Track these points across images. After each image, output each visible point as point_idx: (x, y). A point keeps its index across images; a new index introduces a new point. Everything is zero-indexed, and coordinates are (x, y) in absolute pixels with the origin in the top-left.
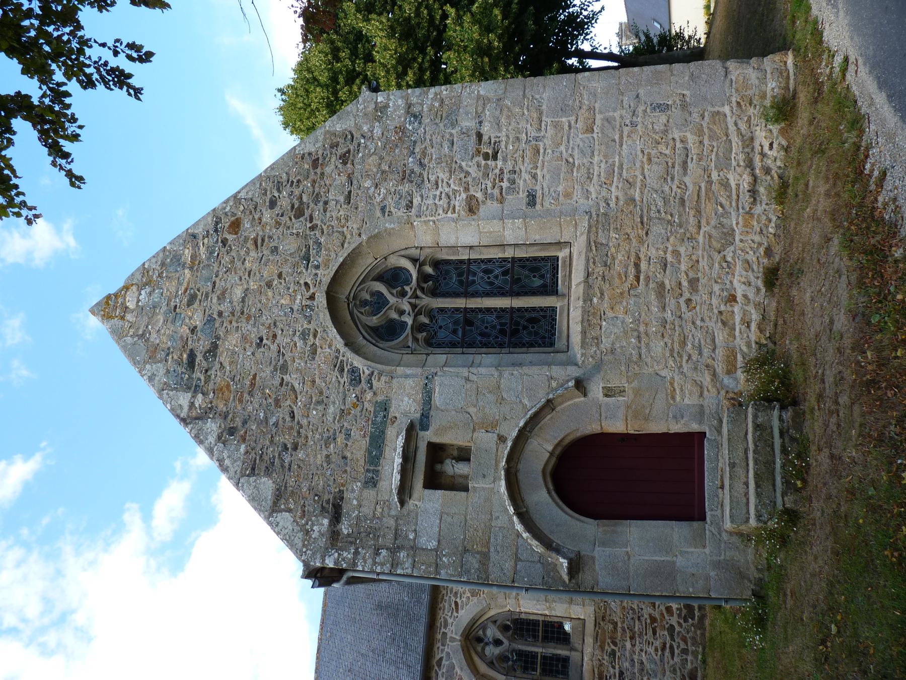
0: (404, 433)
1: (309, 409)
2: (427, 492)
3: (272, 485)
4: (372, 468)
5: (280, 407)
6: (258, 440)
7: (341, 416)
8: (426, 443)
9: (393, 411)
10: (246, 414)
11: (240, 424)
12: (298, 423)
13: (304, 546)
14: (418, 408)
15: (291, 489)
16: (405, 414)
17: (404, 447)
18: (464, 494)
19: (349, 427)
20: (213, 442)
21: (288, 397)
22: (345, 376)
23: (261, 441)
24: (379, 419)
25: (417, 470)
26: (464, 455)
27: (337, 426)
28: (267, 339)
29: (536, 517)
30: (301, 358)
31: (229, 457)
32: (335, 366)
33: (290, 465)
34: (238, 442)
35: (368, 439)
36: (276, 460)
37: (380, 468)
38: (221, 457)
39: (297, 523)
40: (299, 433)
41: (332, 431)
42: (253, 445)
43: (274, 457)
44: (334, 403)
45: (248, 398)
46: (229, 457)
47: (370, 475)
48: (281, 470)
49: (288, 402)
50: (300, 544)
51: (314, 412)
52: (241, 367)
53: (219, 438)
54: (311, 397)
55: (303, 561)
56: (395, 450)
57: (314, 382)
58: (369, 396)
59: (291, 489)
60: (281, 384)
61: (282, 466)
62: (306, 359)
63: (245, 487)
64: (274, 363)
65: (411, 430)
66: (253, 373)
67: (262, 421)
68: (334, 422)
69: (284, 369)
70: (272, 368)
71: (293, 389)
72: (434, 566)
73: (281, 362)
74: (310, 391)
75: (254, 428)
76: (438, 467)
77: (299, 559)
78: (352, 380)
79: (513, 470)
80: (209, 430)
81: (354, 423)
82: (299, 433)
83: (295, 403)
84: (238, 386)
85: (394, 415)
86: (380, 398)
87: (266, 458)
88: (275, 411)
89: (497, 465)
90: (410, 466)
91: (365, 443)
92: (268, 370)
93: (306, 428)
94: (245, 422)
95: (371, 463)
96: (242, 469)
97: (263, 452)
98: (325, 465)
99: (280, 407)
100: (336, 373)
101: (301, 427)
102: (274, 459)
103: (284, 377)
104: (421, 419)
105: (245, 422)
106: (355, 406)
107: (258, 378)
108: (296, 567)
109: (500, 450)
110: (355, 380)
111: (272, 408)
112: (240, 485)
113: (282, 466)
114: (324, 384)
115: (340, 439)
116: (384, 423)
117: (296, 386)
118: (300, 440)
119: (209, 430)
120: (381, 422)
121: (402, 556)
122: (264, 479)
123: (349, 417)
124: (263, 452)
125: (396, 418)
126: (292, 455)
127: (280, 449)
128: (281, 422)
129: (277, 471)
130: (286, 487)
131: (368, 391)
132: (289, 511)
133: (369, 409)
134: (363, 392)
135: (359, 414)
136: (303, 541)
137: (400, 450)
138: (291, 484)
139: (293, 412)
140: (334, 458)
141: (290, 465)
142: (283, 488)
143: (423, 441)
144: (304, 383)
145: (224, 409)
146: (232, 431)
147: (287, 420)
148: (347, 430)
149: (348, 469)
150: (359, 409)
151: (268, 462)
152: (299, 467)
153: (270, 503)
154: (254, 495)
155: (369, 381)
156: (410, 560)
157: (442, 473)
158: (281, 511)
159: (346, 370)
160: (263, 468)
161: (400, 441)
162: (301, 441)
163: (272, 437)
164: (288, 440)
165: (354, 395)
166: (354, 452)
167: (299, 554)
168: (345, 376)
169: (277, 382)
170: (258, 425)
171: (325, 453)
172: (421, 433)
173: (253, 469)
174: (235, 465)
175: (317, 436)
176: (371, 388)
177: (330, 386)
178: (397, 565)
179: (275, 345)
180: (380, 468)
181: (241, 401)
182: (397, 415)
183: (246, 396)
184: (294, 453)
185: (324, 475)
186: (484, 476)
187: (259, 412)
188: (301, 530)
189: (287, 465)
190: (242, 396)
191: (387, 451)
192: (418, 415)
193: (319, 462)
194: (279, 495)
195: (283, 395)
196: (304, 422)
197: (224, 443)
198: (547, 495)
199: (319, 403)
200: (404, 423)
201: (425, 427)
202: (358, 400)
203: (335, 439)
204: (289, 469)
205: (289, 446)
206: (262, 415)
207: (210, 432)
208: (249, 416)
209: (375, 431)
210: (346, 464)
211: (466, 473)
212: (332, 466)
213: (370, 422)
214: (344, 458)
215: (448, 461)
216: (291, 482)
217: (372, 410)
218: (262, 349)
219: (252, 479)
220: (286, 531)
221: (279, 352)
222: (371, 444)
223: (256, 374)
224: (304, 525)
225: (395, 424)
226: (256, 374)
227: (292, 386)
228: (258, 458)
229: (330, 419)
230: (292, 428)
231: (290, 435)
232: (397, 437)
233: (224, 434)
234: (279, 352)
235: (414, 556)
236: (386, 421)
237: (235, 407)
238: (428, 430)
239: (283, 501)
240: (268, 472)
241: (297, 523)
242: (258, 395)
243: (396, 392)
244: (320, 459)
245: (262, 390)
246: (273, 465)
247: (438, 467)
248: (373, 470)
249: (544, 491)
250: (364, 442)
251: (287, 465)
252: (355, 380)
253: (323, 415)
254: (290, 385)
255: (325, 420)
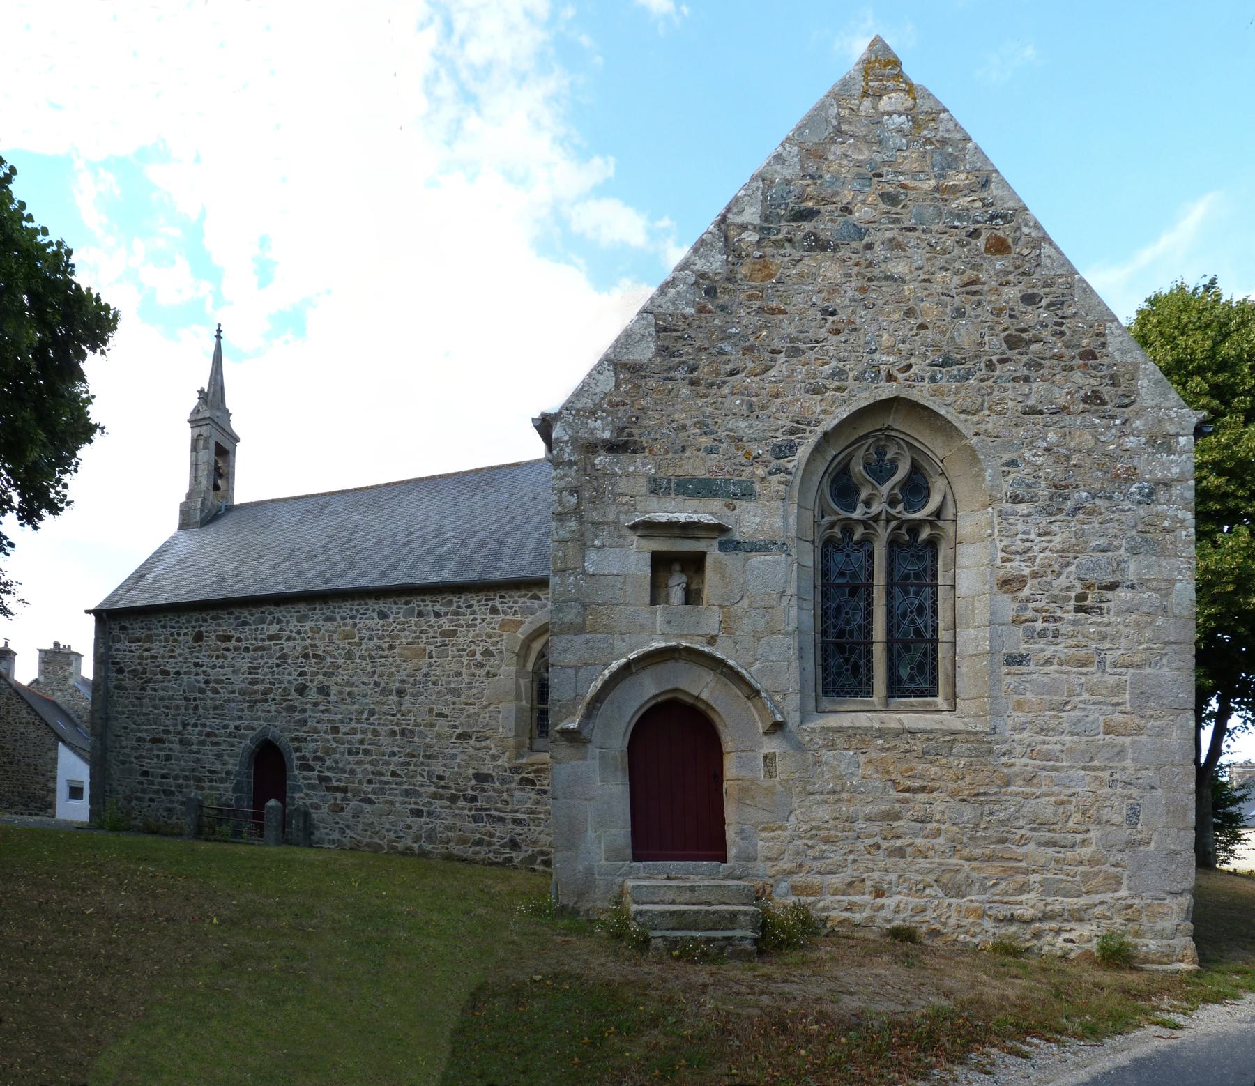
0: (716, 521)
1: (743, 394)
2: (648, 556)
3: (646, 358)
4: (672, 485)
5: (744, 354)
6: (701, 330)
7: (734, 438)
8: (705, 550)
9: (741, 505)
10: (734, 309)
11: (720, 302)
12: (724, 382)
13: (578, 410)
14: (746, 536)
15: (643, 384)
16: (738, 521)
17: (699, 523)
18: (648, 600)
19: (720, 450)
20: (697, 267)
21: (758, 363)
22: (785, 437)
23: (700, 335)
24: (731, 488)
25: (673, 541)
26: (692, 596)
27: (722, 434)
28: (833, 322)
29: (627, 682)
30: (808, 373)
31: (678, 293)
32: (798, 422)
33: (671, 379)
34: (698, 303)
35: (707, 476)
36: (677, 359)
37: (673, 496)
38: (678, 283)
39: (603, 399)
40: (712, 384)
41: (715, 428)
42: (695, 324)
43: (680, 356)
44: (750, 427)
45: (755, 307)
46: (678, 293)
47: (664, 484)
48: (665, 368)
49: (750, 365)
50: (579, 406)
51: (738, 402)
52: (795, 290)
53: (702, 276)
54: (757, 395)
55: (560, 413)
56: (695, 512)
57: (777, 396)
58: (761, 472)
59: (643, 384)
60: (773, 352)
61: (670, 369)
62: (807, 381)
63: (642, 322)
64: (801, 336)
65: (720, 529)
66: (788, 308)
67: (725, 331)
68: (727, 430)
69: (794, 352)
70: (795, 335)
71: (768, 369)
72: (563, 567)
73: (803, 347)
74: (765, 392)
75: (716, 322)
76: (677, 567)
77: (562, 407)
78: (780, 447)
79: (677, 655)
80: (712, 259)
81: (726, 457)
82: (712, 384)
83: (750, 375)
84: (770, 291)
85: (737, 506)
86: (758, 487)
87: (679, 345)
88: (738, 348)
89: (682, 636)
90: (677, 532)
91: (702, 473)
92: (791, 330)
93: (719, 394)
94: (723, 308)
95: (678, 484)
96: (664, 314)
97: (686, 339)
98: (674, 425)
99: (744, 354)
100: (789, 425)
101: (719, 387)
102: (678, 356)
103: (783, 355)
104: (733, 541)
105: (723, 308)
106: (747, 455)
107: (781, 317)
108: (553, 404)
109: (700, 638)
110: (781, 451)
111: (743, 344)
112: (645, 315)
113: (670, 369)
114: (774, 410)
115: (706, 441)
116: (727, 494)
117: (771, 373)
118: (703, 387)
119: (712, 259)
120: (728, 492)
121: (572, 524)
122: (652, 346)
123: (733, 449)
124: (686, 339)
125: (734, 509)
126: (684, 379)
127: (691, 362)
128: (725, 358)
129: (664, 363)
130: (645, 377)
131: (766, 470)
132: (617, 387)
133: (744, 474)
134: (765, 464)
135: (737, 461)
136: (583, 409)
137: (695, 518)
138: (649, 384)
139: (738, 373)
140: (682, 436)
141: (671, 379)
142: (643, 374)
143: (707, 547)
144: (775, 382)
145: (739, 276)
146: (711, 292)
147: (728, 367)
148: (717, 448)
149: (670, 456)
150: (744, 461)
151: (674, 349)
152: (670, 392)
153: (625, 359)
154: (634, 336)
155: (778, 470)
156: (568, 536)
157: (670, 572)
158: (616, 375)
159: (793, 437)
160: (666, 343)
161: (705, 518)
162: (702, 390)
163: (706, 349)
164: (703, 372)
165: (760, 452)
166: (691, 461)
167: (568, 406)
168: (785, 437)
169: (776, 345)
170: (720, 327)
171: (688, 423)
172: (716, 543)
173: (665, 330)
174: (669, 304)
175: (708, 410)
176: (771, 473)
177: (772, 419)
178: (561, 520)
179: (826, 335)
180: (673, 496)
181: (750, 298)
182: (737, 510)
183: (756, 304)
184: (687, 381)
185: (662, 425)
186: (669, 622)
187: (737, 326)
188: (595, 405)
189: (672, 374)
190: (757, 298)
191: (693, 503)
192: (737, 537)
193: (676, 417)
194: (634, 369)
195: (760, 356)
196: (726, 390)
197: (696, 284)
198: (651, 695)
199: (751, 407)
200: (728, 521)
201: (723, 547)
202: (754, 458)
203: (705, 433)
204: (667, 379)
205: (695, 373)
206: (733, 330)
207: (709, 261)
208: (731, 314)
209: (717, 485)
210: (676, 452)
211: (672, 601)
212: (673, 434)
213: (727, 477)
214: (683, 449)
215: (684, 578)
216: (652, 384)
217: (743, 478)
218: (819, 317)
219: (652, 330)
220: (593, 386)
221: (817, 342)
222: (701, 481)
223: (786, 313)
224: (601, 406)
225: (725, 509)
226: (786, 313)
227: (771, 367)
228: (679, 334)
229: (730, 425)
230: (717, 374)
231: (709, 373)
232: (711, 514)
233: (707, 282)
234: (817, 342)
235: (572, 540)
236: (729, 497)
237: (742, 291)
238: (720, 550)
239: (628, 376)
240: (663, 351)
241: (603, 399)
242: (757, 321)
243: (765, 506)
244: (680, 417)
245: (766, 326)
246: (670, 356)
247: (677, 567)
248: (670, 487)
249: (654, 692)
250: (703, 472)
251: (672, 374)
252: (781, 451)
253: (735, 414)
254: (773, 363)
255: (728, 418)
